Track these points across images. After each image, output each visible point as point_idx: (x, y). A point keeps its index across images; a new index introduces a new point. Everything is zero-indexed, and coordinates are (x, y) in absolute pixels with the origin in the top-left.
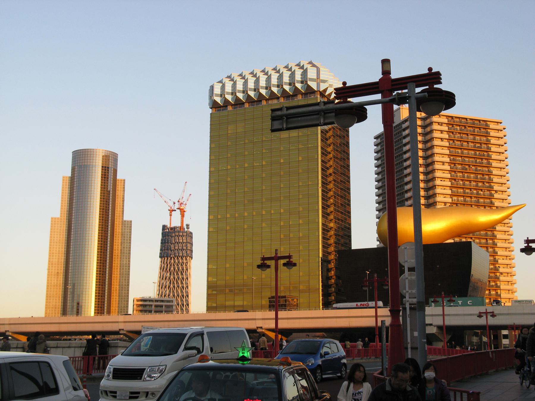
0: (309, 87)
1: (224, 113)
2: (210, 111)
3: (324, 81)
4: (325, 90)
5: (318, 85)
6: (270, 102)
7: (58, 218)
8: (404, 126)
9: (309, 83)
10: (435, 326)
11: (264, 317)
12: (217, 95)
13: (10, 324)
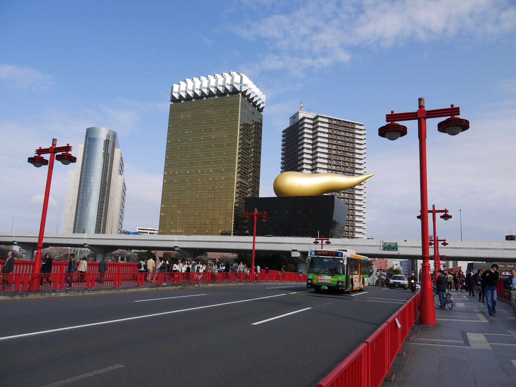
0: (234, 88)
1: (178, 104)
3: (246, 85)
4: (246, 92)
5: (241, 87)
6: (209, 98)
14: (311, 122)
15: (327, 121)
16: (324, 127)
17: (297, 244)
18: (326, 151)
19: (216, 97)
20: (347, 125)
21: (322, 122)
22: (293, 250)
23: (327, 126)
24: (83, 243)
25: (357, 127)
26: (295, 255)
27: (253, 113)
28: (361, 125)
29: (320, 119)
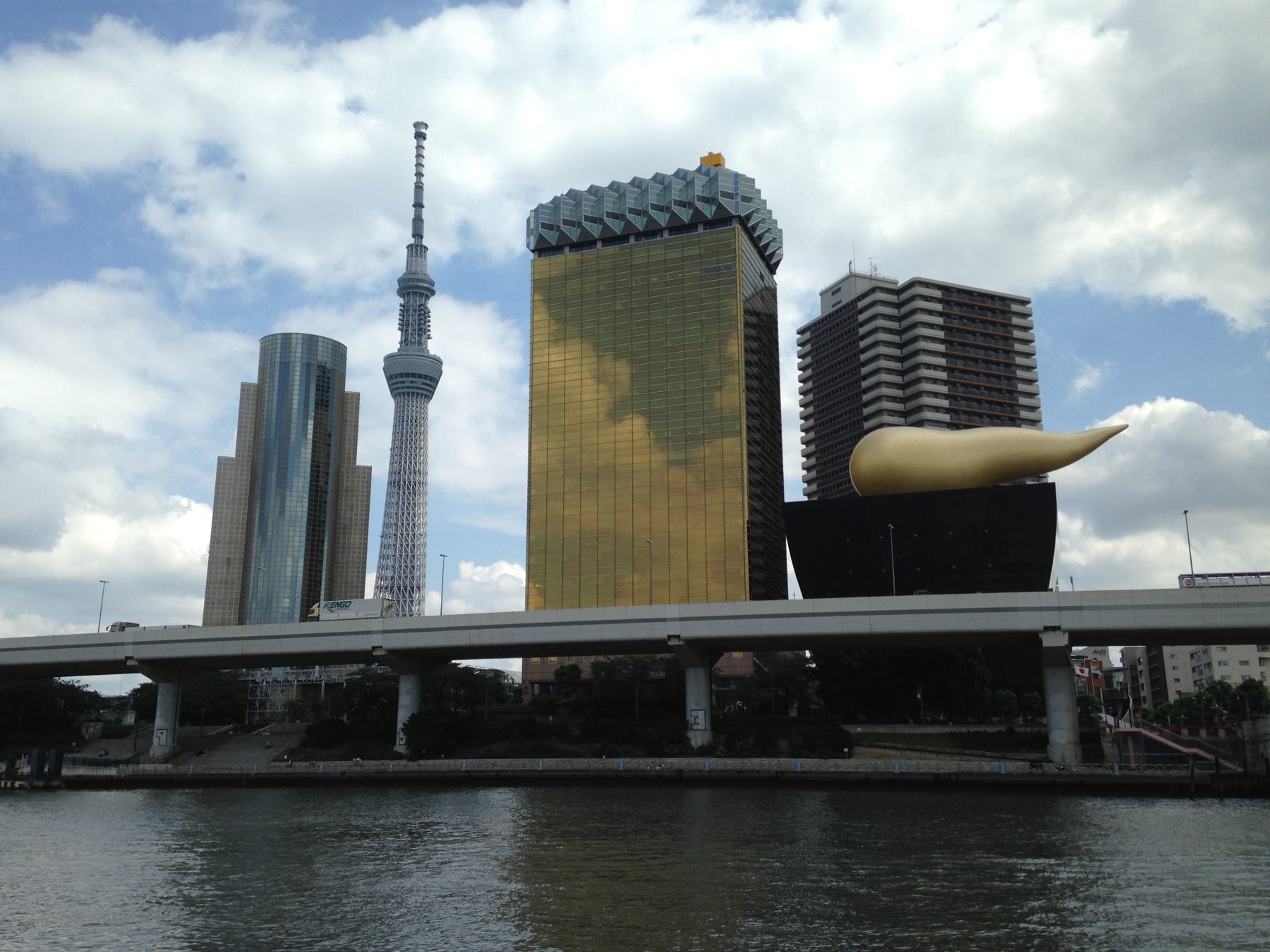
2: (532, 255)
3: (745, 199)
4: (748, 217)
7: (231, 459)
8: (861, 305)
9: (722, 200)
10: (1064, 632)
11: (683, 615)
13: (135, 643)
15: (938, 294)
17: (1059, 609)
19: (666, 235)
20: (989, 304)
22: (1047, 629)
23: (939, 307)
24: (369, 647)
25: (1015, 307)
26: (1049, 641)
27: (762, 277)
28: (1024, 302)
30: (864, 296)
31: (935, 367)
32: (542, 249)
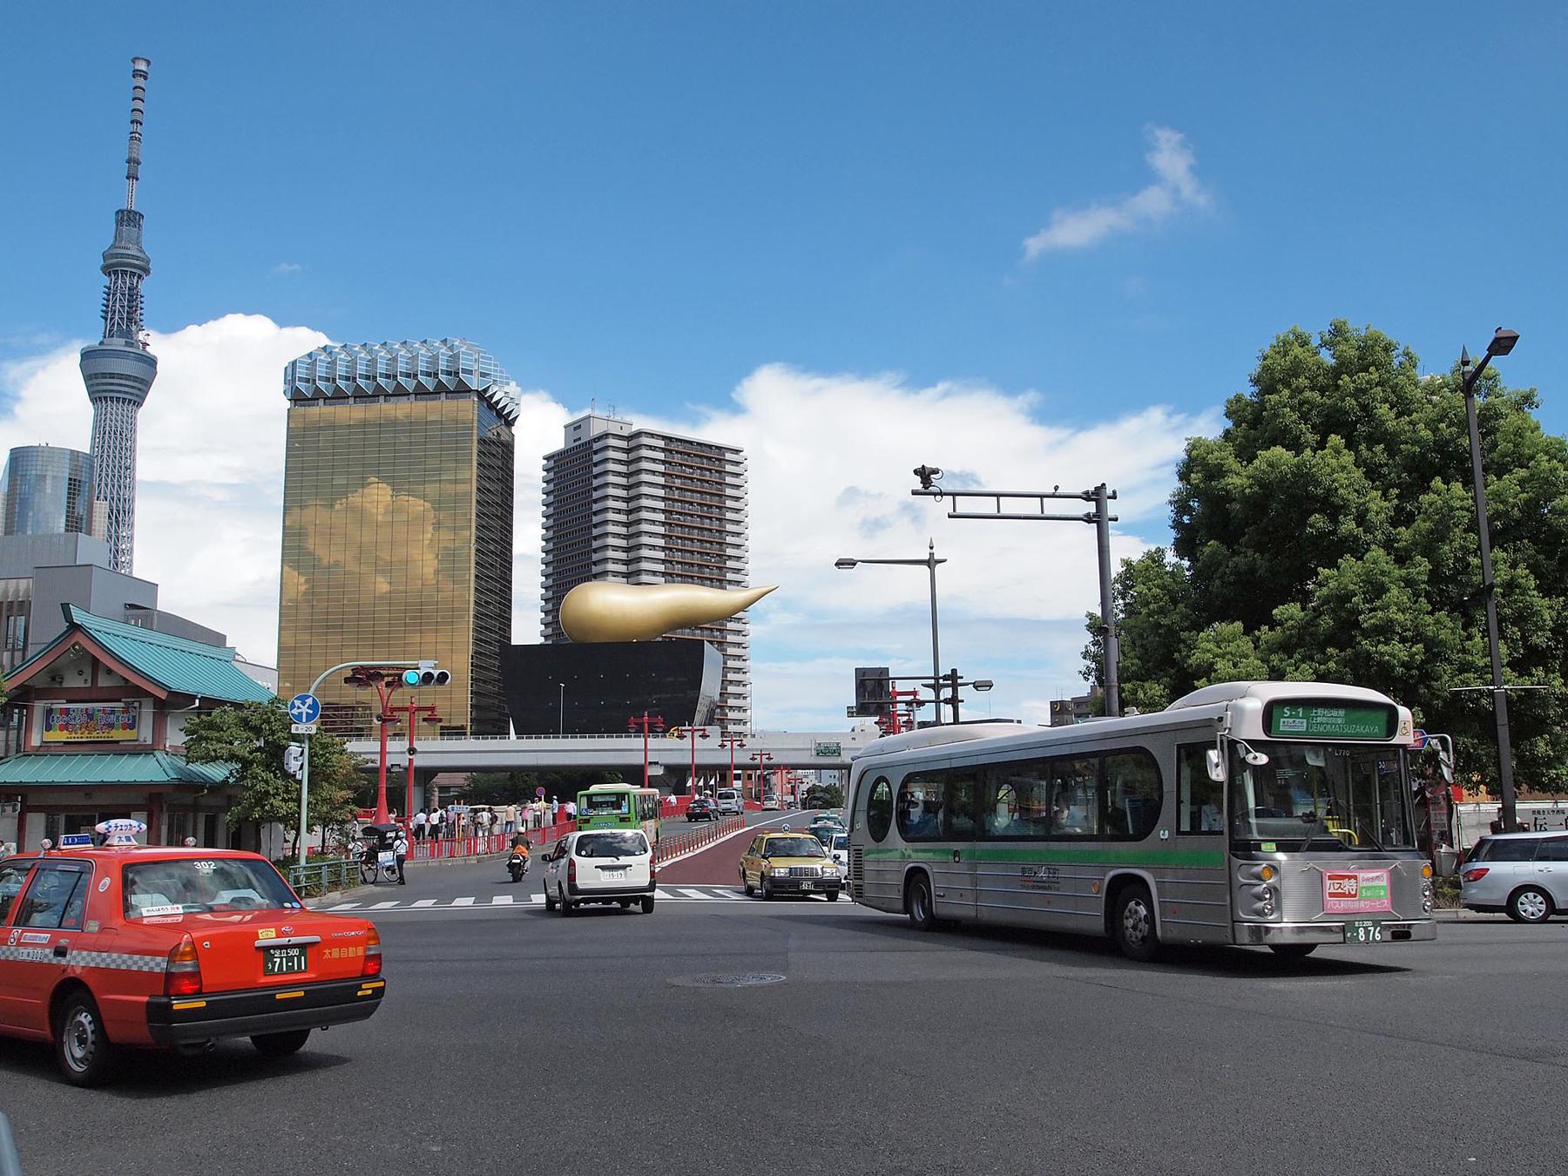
2: (288, 404)
4: (485, 390)
8: (596, 446)
12: (300, 379)
14: (623, 444)
15: (661, 444)
16: (654, 460)
18: (661, 517)
21: (651, 448)
23: (661, 456)
25: (728, 456)
28: (737, 452)
29: (645, 440)
30: (599, 438)
31: (654, 510)
32: (297, 398)
